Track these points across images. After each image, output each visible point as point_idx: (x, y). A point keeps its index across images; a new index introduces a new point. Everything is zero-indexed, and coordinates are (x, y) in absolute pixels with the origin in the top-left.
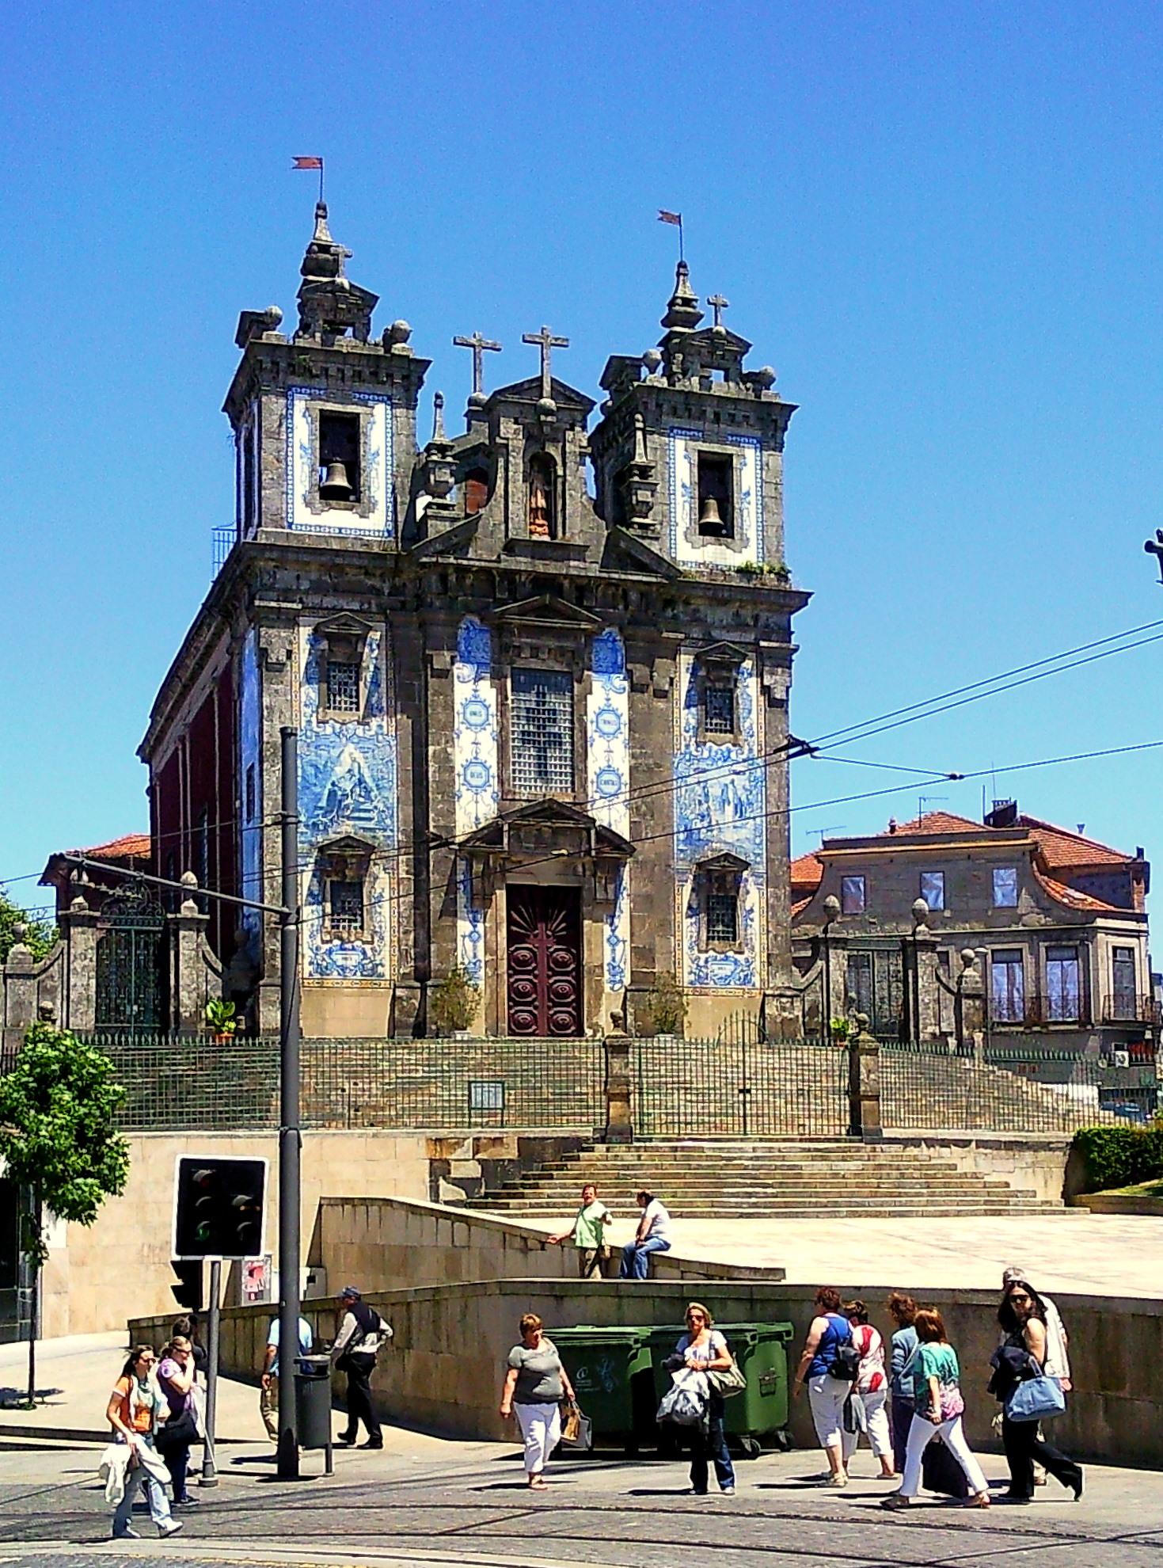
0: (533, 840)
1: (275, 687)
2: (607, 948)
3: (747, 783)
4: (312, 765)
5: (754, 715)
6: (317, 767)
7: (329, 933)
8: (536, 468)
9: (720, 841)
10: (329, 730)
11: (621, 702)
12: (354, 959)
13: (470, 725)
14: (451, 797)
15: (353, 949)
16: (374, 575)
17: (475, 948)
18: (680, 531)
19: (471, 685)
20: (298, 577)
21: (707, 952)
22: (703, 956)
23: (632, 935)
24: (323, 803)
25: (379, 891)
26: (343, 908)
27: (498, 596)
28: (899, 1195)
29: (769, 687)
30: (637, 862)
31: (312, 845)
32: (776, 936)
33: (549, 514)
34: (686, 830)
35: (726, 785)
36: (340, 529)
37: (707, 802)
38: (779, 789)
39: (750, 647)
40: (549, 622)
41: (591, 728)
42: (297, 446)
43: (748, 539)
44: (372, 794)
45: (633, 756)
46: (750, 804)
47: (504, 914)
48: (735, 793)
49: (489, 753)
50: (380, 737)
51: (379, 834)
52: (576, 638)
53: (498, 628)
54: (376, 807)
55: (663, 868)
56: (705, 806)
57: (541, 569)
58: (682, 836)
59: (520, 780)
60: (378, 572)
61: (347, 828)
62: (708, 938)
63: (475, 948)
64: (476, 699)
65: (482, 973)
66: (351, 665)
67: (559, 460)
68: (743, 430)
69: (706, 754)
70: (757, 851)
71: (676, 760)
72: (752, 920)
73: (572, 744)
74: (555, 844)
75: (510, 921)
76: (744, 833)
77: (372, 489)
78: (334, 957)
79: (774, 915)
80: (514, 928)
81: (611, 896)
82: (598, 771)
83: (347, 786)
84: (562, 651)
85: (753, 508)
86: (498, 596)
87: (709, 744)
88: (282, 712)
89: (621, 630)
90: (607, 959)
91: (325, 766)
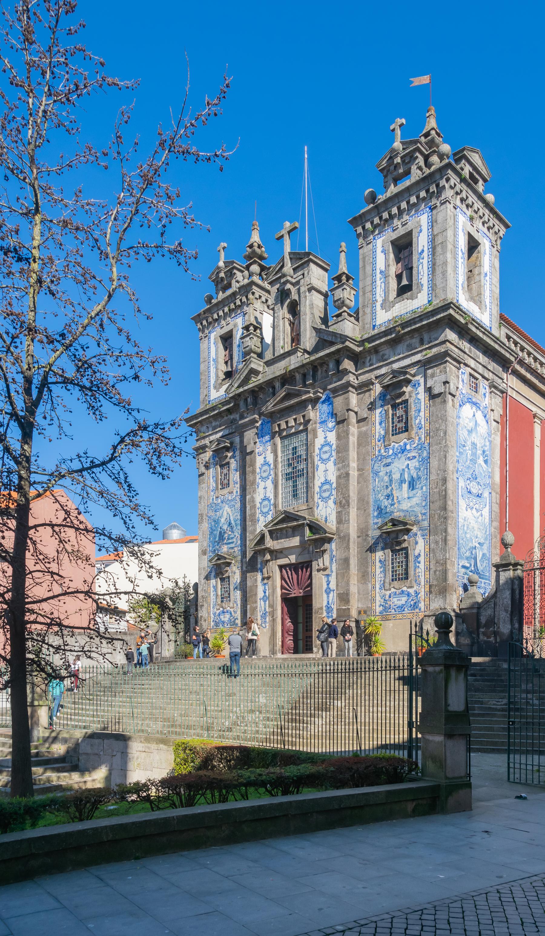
9: (399, 510)
24: (217, 539)
30: (340, 538)
35: (403, 470)
37: (391, 486)
48: (409, 474)
55: (364, 538)
56: (390, 488)
69: (391, 452)
72: (419, 563)
76: (415, 500)
83: (225, 527)
87: (393, 444)
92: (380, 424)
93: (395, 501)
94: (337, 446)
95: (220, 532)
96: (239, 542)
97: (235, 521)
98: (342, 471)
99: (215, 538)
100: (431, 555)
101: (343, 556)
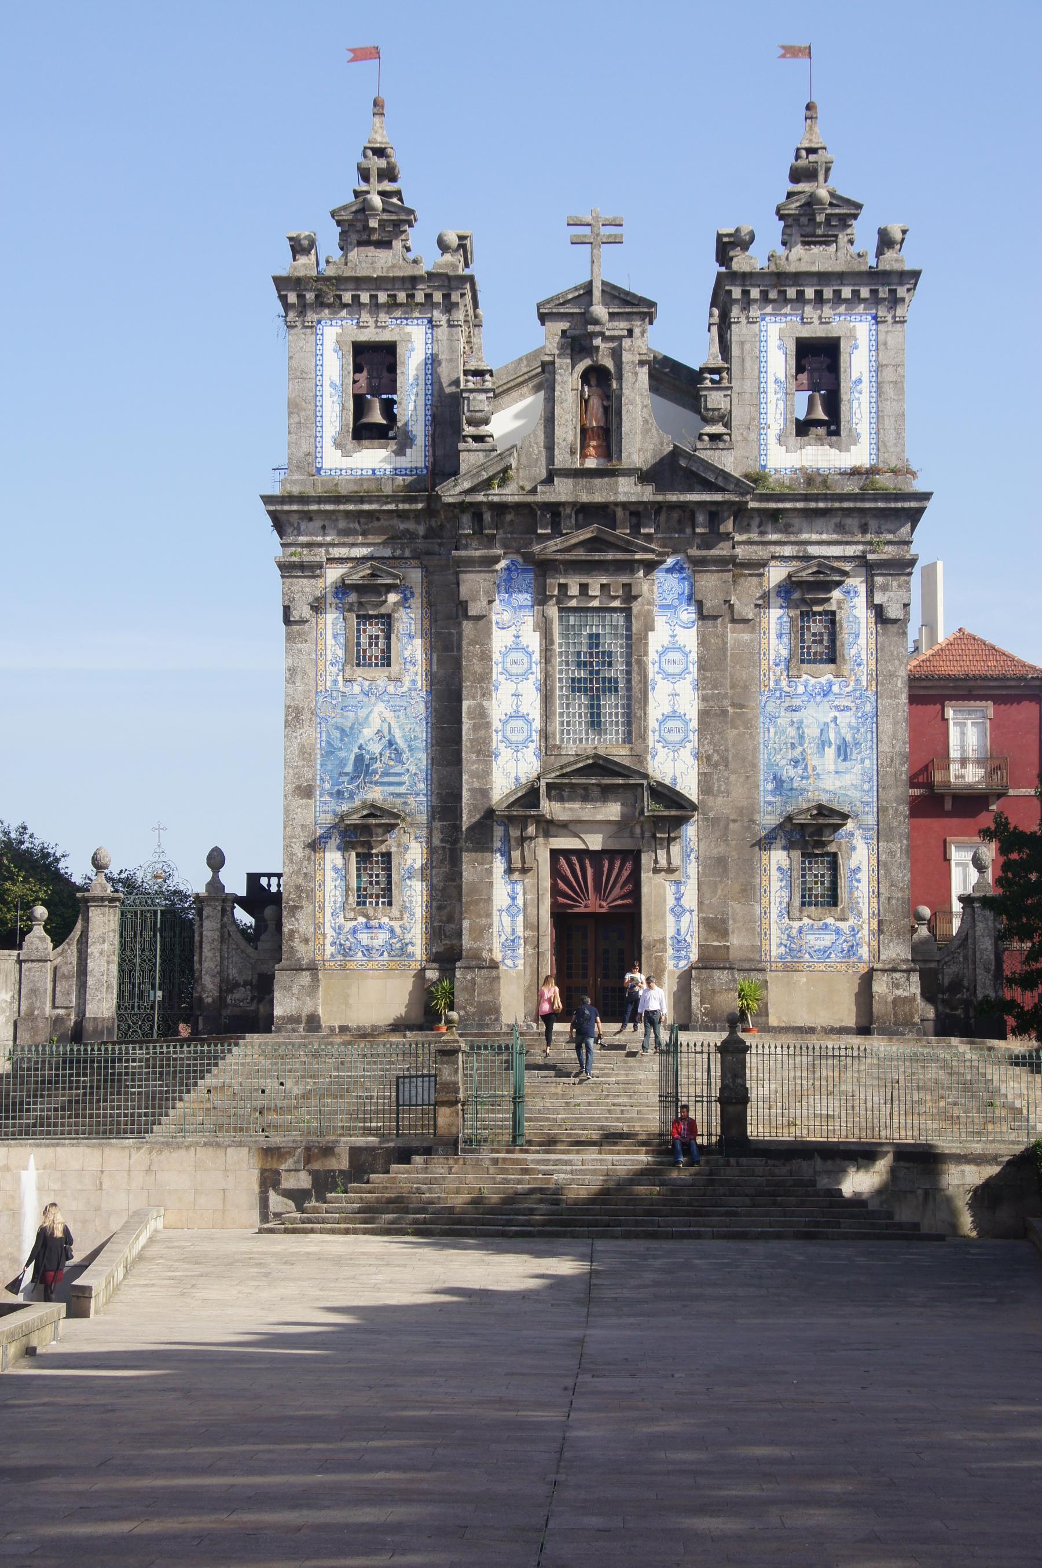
1: (299, 646)
2: (670, 919)
3: (853, 720)
4: (337, 728)
5: (862, 641)
7: (353, 910)
8: (593, 382)
9: (819, 789)
10: (357, 689)
11: (689, 638)
12: (381, 938)
13: (510, 676)
14: (486, 754)
15: (380, 927)
16: (408, 518)
17: (513, 921)
18: (772, 436)
19: (512, 631)
20: (324, 527)
21: (801, 919)
22: (796, 924)
23: (700, 903)
24: (349, 768)
25: (409, 862)
26: (371, 883)
27: (539, 531)
28: (708, 1214)
29: (881, 605)
30: (707, 819)
31: (335, 813)
32: (889, 899)
34: (775, 778)
35: (826, 724)
36: (374, 471)
37: (801, 745)
38: (895, 723)
40: (597, 556)
41: (652, 671)
43: (858, 434)
45: (704, 699)
46: (857, 744)
47: (547, 883)
48: (838, 732)
49: (532, 704)
50: (413, 694)
51: (411, 800)
53: (544, 568)
56: (800, 749)
57: (585, 498)
58: (770, 787)
59: (568, 733)
60: (412, 515)
61: (375, 794)
62: (803, 904)
63: (513, 921)
64: (517, 647)
65: (521, 951)
66: (382, 616)
69: (801, 689)
70: (866, 799)
72: (859, 881)
73: (629, 689)
75: (555, 891)
76: (848, 779)
78: (359, 936)
79: (888, 872)
80: (561, 900)
82: (660, 718)
85: (865, 398)
87: (805, 677)
90: (670, 932)
91: (352, 728)
92: (780, 636)
93: (810, 772)
94: (701, 658)
95: (359, 759)
96: (422, 786)
97: (409, 741)
98: (711, 703)
100: (882, 872)
101: (715, 853)
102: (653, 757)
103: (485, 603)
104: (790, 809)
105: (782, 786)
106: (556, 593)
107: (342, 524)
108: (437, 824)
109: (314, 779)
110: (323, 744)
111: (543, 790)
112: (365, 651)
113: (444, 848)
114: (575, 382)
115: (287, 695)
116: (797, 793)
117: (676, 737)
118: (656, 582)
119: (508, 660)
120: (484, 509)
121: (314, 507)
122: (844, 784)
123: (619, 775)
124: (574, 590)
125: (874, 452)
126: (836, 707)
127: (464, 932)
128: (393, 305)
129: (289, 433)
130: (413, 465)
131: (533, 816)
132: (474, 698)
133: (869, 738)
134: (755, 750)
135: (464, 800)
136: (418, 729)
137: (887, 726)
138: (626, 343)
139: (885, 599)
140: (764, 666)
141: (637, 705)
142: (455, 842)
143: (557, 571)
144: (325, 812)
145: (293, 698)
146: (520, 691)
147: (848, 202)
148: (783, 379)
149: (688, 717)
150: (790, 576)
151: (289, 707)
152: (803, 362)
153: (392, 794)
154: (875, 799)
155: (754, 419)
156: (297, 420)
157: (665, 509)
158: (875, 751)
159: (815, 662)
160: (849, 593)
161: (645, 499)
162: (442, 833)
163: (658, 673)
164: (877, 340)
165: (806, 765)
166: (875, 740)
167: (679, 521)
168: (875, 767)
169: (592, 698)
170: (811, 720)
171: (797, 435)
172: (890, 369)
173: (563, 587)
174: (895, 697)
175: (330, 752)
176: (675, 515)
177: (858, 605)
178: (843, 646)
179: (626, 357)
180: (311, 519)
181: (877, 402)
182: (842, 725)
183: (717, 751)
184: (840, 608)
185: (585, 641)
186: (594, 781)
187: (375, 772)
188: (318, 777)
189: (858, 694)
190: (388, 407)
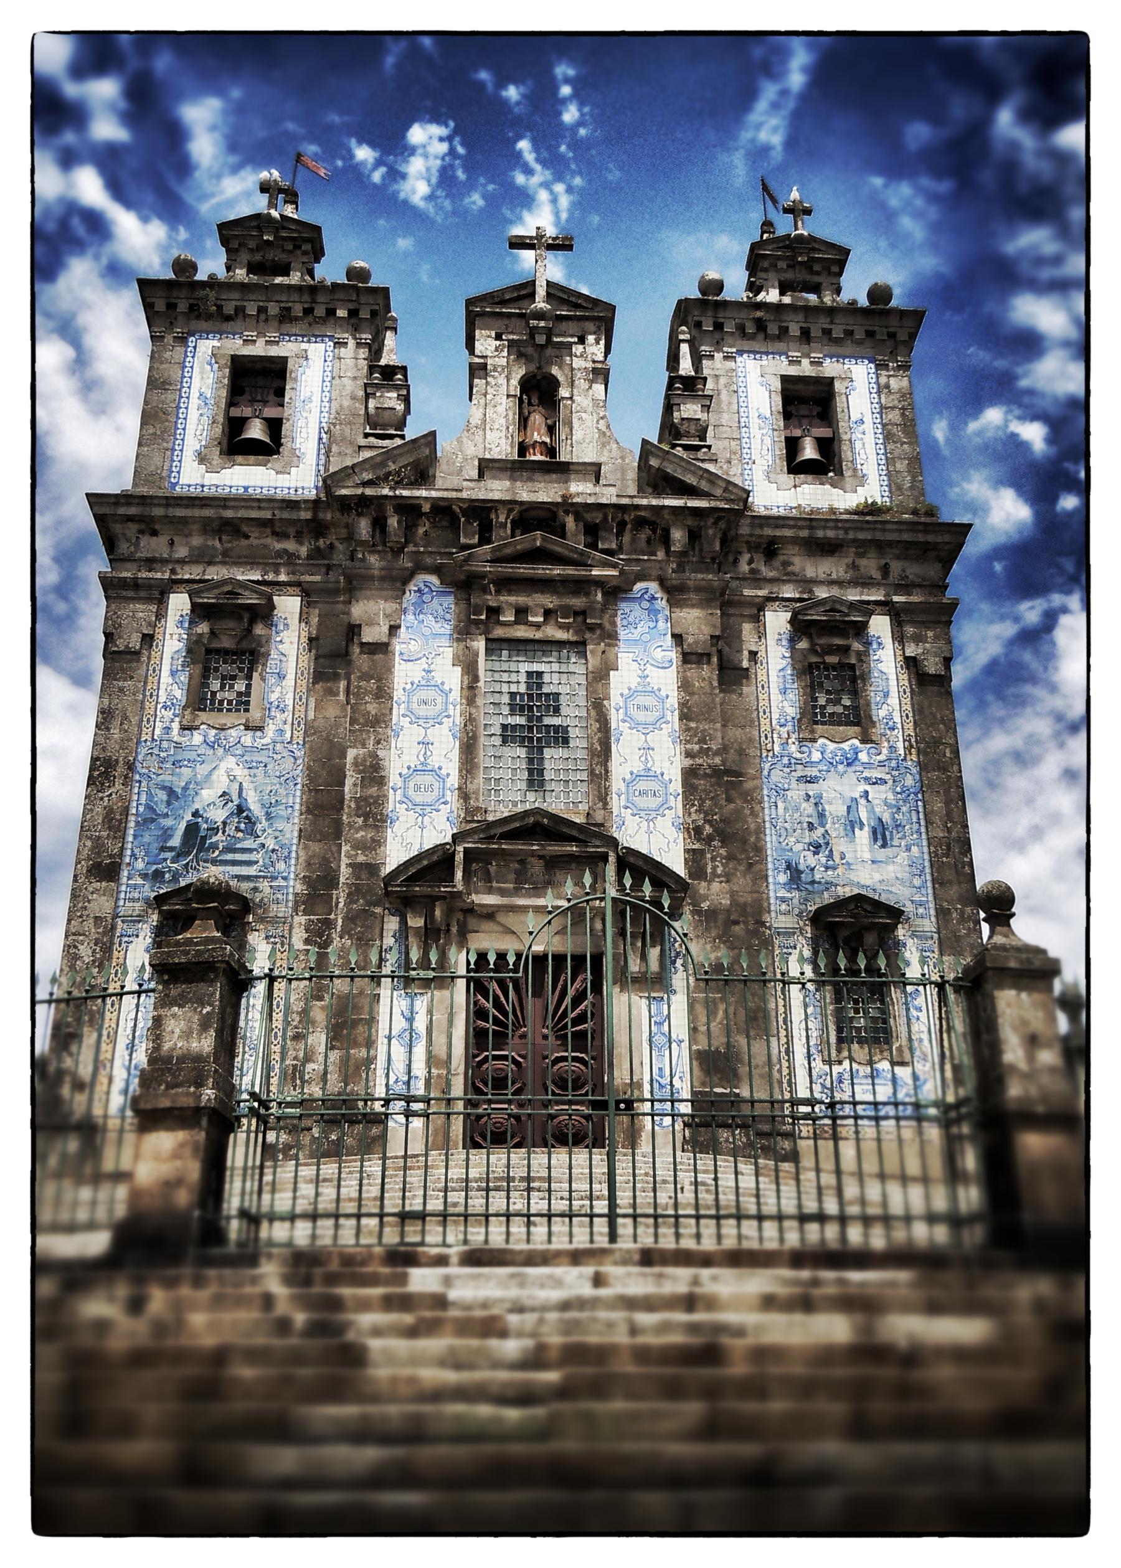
0: (512, 876)
1: (120, 684)
3: (890, 796)
4: (164, 788)
5: (894, 700)
6: (171, 792)
8: (535, 401)
9: (851, 884)
13: (416, 720)
20: (172, 543)
23: (693, 1030)
24: (176, 841)
27: (463, 540)
29: (914, 659)
30: (697, 912)
31: (147, 901)
33: (552, 451)
34: (789, 867)
36: (246, 488)
38: (947, 803)
39: (879, 609)
41: (615, 719)
42: (194, 395)
44: (259, 827)
45: (689, 754)
46: (900, 825)
48: (871, 811)
50: (279, 747)
51: (264, 885)
52: (587, 594)
54: (263, 845)
56: (821, 831)
57: (525, 496)
58: (783, 878)
60: (292, 531)
62: (840, 1040)
64: (428, 682)
66: (243, 653)
67: (561, 378)
68: (849, 348)
69: (816, 756)
70: (916, 898)
71: (767, 766)
74: (549, 883)
76: (891, 871)
77: (298, 441)
81: (654, 965)
82: (628, 777)
84: (566, 611)
86: (463, 540)
87: (821, 741)
88: (125, 718)
89: (662, 582)
92: (784, 692)
94: (683, 705)
95: (192, 829)
98: (699, 761)
99: (165, 841)
102: (619, 828)
103: (385, 629)
104: (813, 908)
105: (799, 878)
106: (483, 617)
107: (197, 541)
108: (301, 919)
109: (121, 854)
110: (141, 809)
111: (459, 857)
112: (214, 694)
113: (308, 951)
114: (512, 388)
115: (95, 744)
116: (822, 887)
117: (652, 802)
118: (619, 613)
119: (415, 699)
120: (390, 510)
121: (158, 512)
122: (885, 877)
123: (571, 839)
124: (508, 617)
125: (887, 494)
126: (866, 779)
127: (330, 1069)
128: (286, 317)
129: (140, 445)
130: (299, 485)
131: (442, 898)
132: (364, 745)
133: (915, 820)
134: (760, 831)
135: (342, 880)
136: (282, 791)
137: (938, 805)
138: (578, 349)
139: (920, 651)
140: (765, 726)
141: (596, 759)
142: (326, 944)
143: (485, 590)
144: (133, 900)
145: (104, 749)
146: (432, 740)
147: (833, 246)
148: (768, 415)
149: (666, 777)
150: (792, 622)
151: (98, 759)
152: (789, 409)
153: (237, 876)
154: (931, 898)
155: (735, 453)
156: (151, 431)
157: (629, 526)
158: (924, 836)
159: (832, 723)
160: (870, 644)
161: (604, 501)
162: (307, 931)
163: (624, 721)
164: (877, 383)
165: (831, 851)
166: (923, 823)
167: (649, 541)
168: (926, 857)
169: (530, 749)
170: (833, 795)
171: (789, 473)
172: (897, 412)
173: (494, 612)
174: (945, 770)
175: (149, 819)
176: (643, 536)
177: (883, 658)
178: (868, 704)
179: (577, 363)
180: (154, 533)
181: (884, 444)
182: (876, 802)
183: (710, 822)
184: (862, 661)
185: (523, 678)
186: (535, 848)
187: (214, 846)
188: (129, 852)
189: (894, 764)
190: (275, 426)
